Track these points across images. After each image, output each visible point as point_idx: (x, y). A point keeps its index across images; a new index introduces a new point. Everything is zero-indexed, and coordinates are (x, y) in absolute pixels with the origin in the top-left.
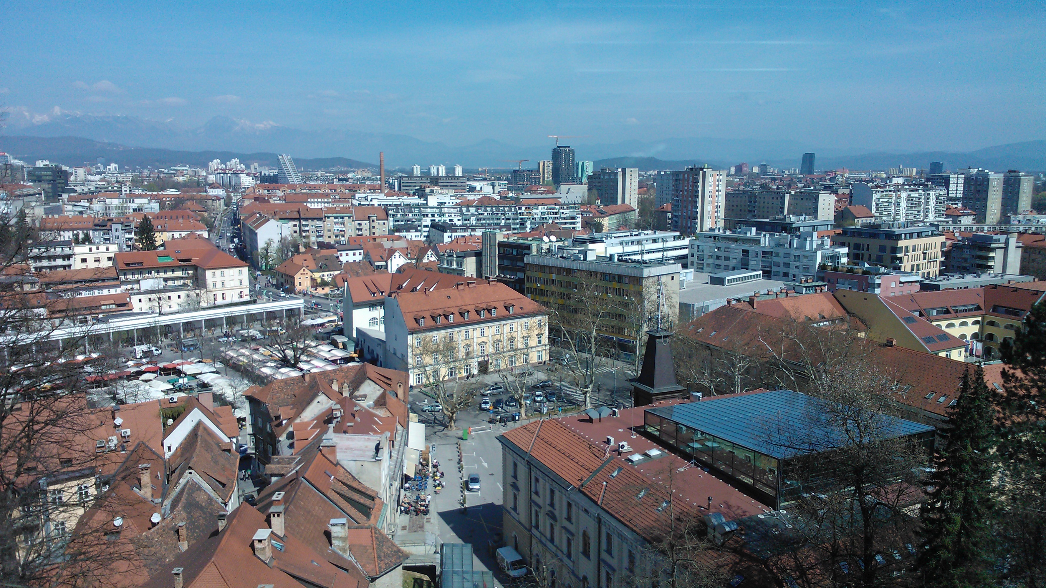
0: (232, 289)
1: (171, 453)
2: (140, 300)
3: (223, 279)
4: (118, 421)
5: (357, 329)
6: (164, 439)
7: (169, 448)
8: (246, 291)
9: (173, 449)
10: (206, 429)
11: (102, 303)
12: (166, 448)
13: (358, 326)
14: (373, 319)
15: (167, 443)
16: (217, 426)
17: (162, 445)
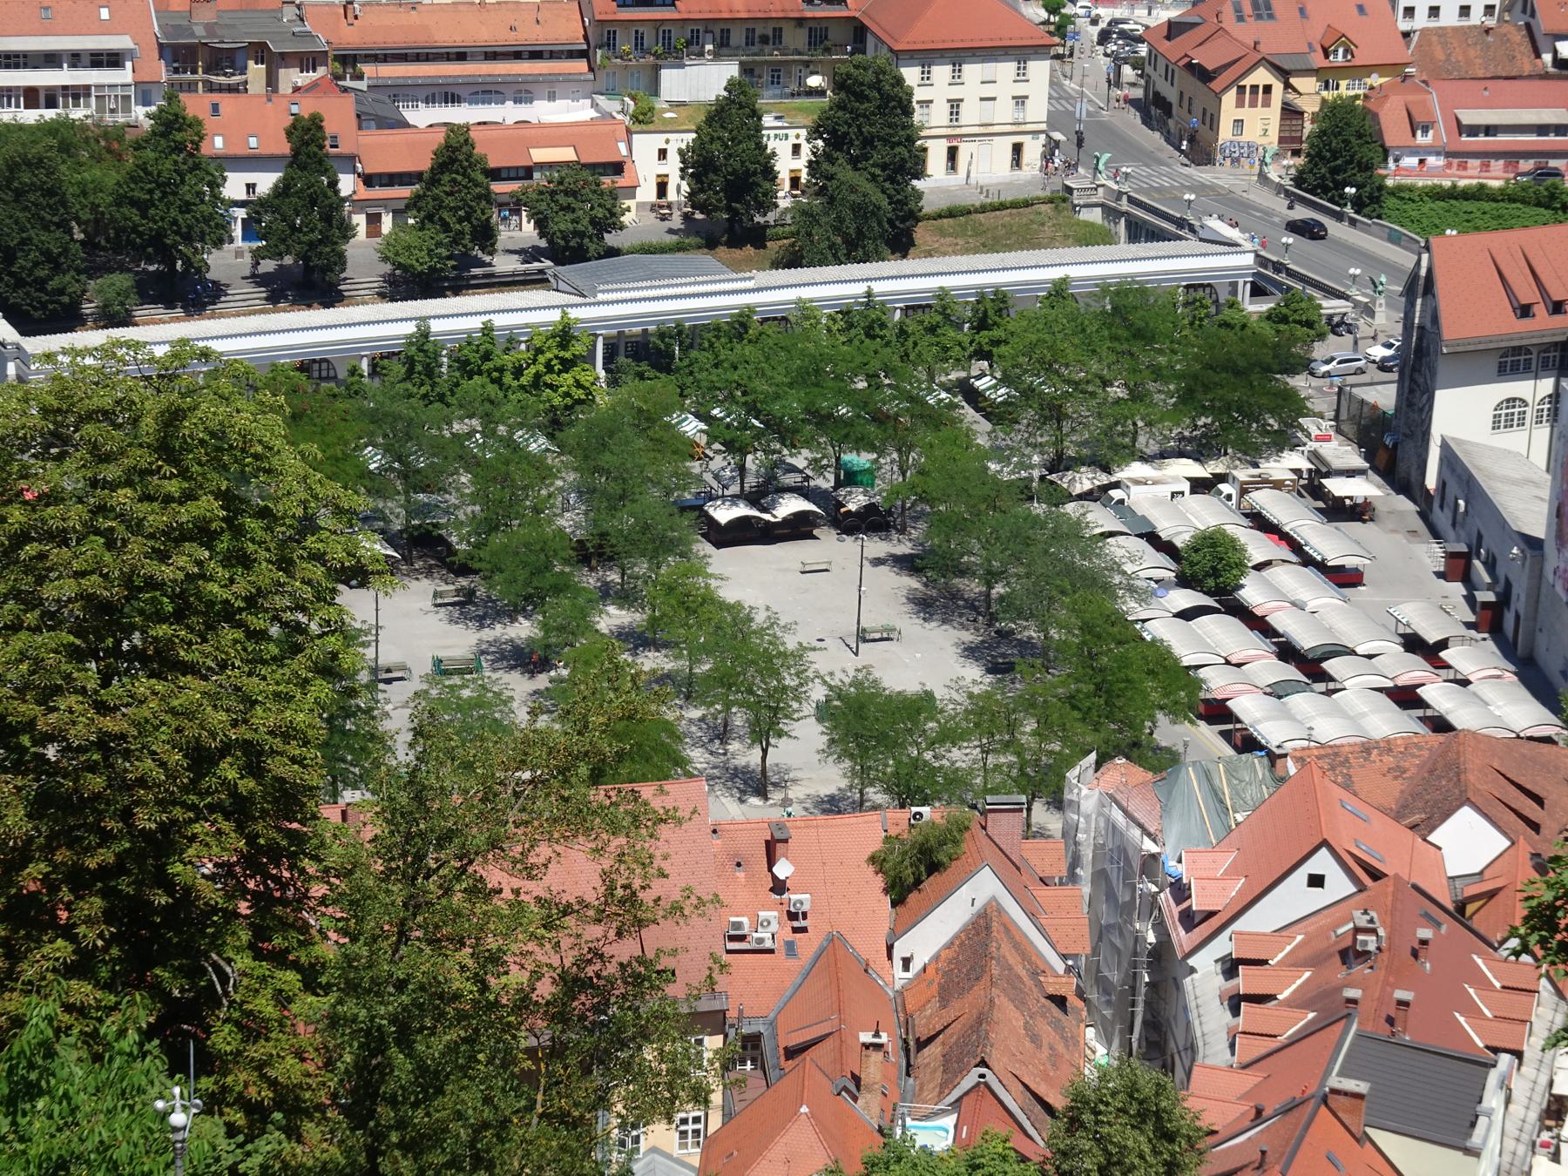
0: (986, 133)
1: (909, 975)
2: (663, 154)
3: (955, 93)
4: (783, 869)
5: (1445, 446)
6: (895, 934)
7: (906, 963)
8: (1033, 151)
9: (916, 966)
10: (1009, 928)
11: (539, 155)
12: (898, 964)
13: (1449, 433)
14: (1511, 401)
15: (900, 950)
16: (1032, 916)
17: (890, 949)
